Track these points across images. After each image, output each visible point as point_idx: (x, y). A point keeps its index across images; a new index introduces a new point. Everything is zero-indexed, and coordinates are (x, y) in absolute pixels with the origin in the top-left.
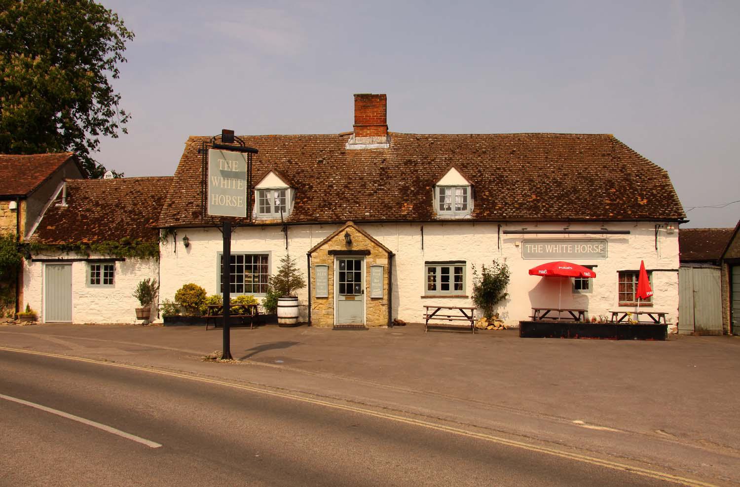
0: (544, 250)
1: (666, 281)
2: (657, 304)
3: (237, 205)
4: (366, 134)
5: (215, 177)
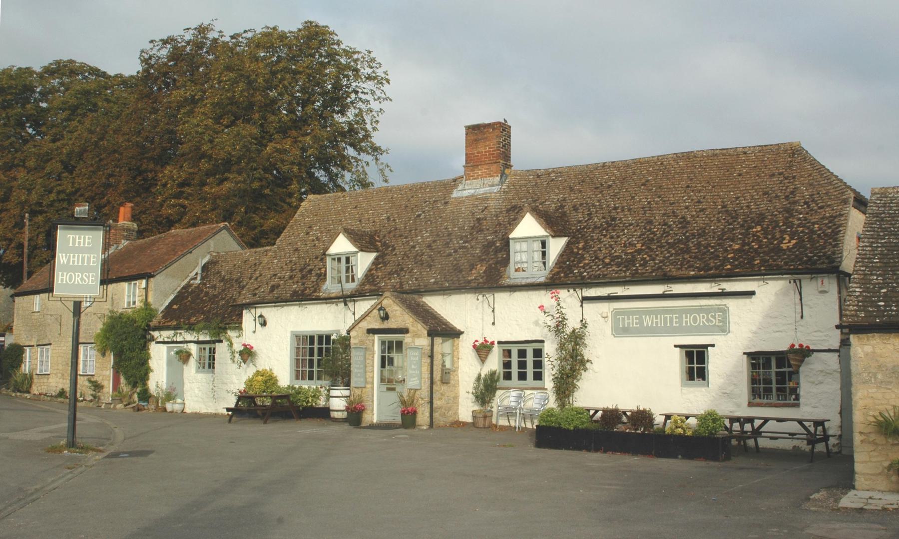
0: (641, 323)
1: (820, 369)
2: (806, 405)
3: (89, 282)
4: (477, 176)
5: (64, 255)
